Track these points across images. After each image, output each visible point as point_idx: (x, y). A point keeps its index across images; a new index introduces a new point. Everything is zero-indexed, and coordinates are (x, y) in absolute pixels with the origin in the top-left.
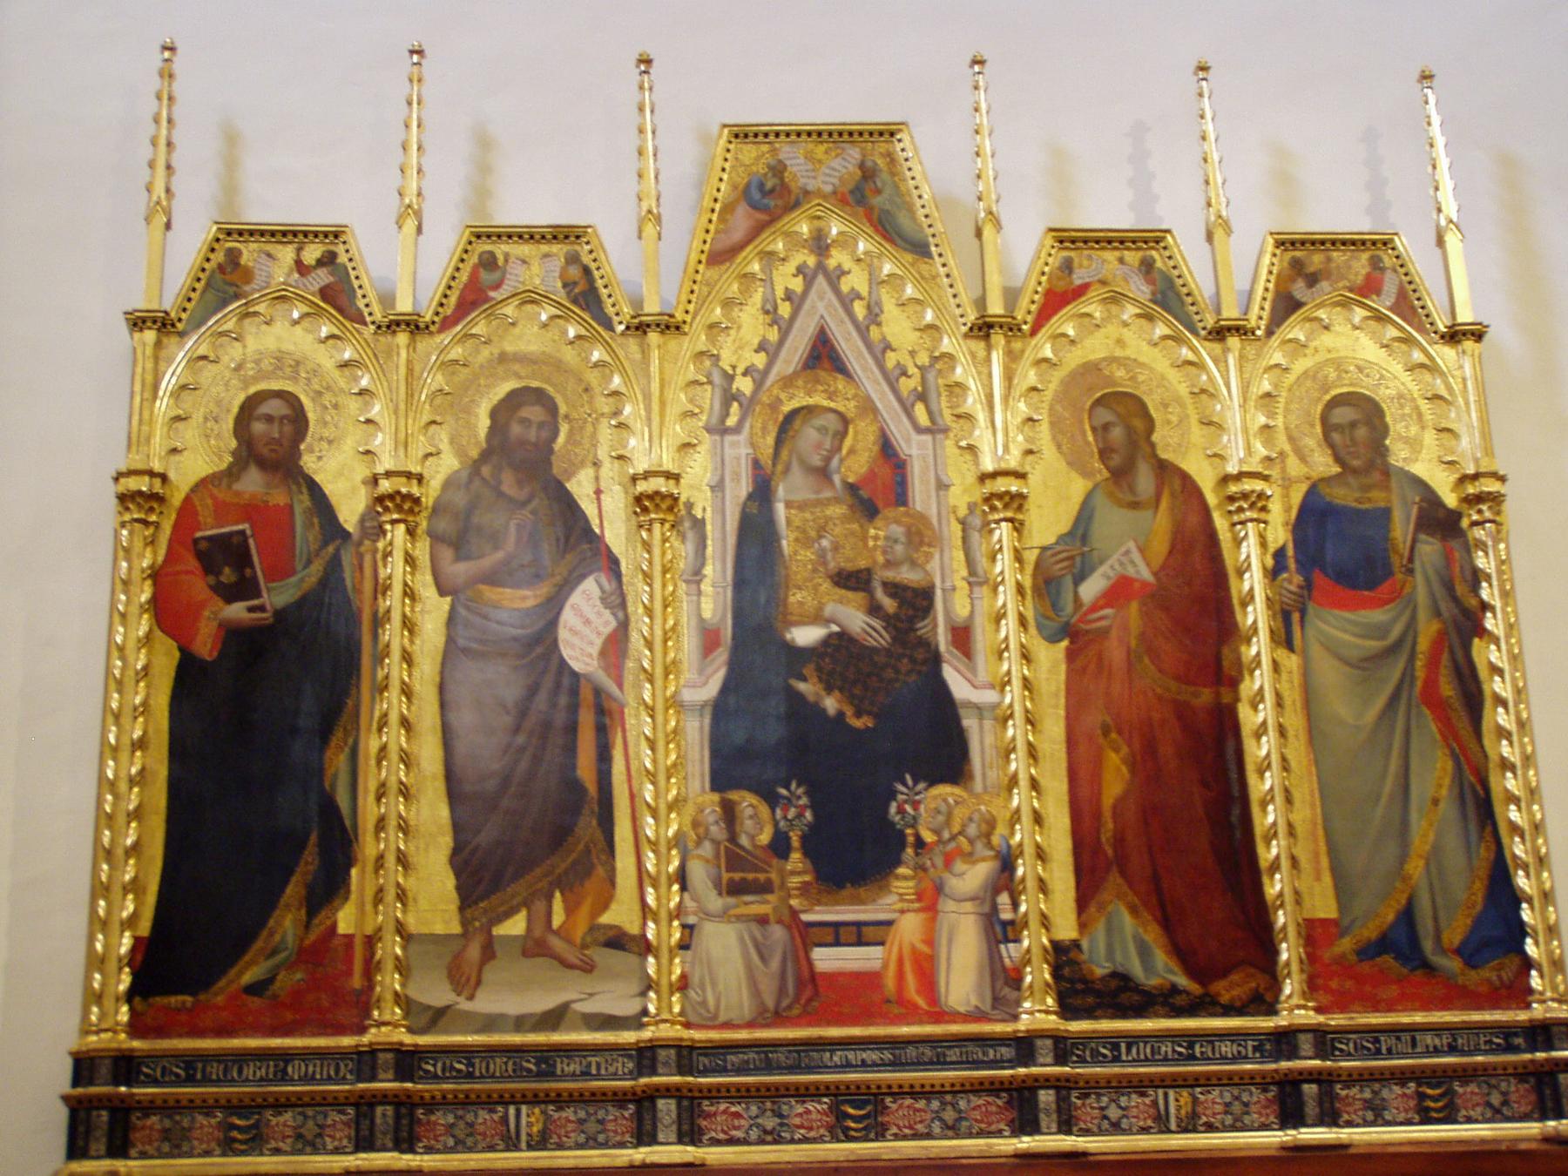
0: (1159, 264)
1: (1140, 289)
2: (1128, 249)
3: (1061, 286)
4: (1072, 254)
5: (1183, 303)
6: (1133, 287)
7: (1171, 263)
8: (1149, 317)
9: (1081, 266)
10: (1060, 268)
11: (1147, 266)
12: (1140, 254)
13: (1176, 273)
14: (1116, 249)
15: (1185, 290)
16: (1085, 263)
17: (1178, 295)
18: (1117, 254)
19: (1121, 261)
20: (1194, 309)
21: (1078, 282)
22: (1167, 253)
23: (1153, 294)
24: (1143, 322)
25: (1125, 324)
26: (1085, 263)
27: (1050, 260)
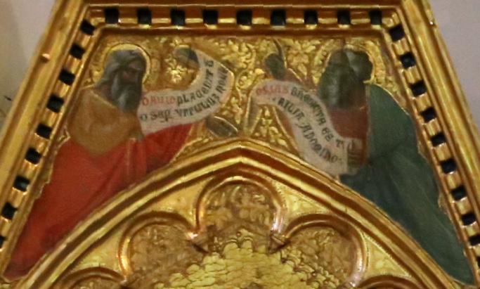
0: (379, 74)
1: (318, 144)
2: (300, 34)
3: (102, 137)
4: (142, 48)
5: (436, 187)
6: (301, 142)
7: (411, 75)
8: (343, 229)
9: (163, 81)
10: (105, 87)
11: (348, 84)
12: (330, 46)
13: (423, 101)
14: (260, 32)
15: (442, 152)
16: (176, 73)
17: (423, 162)
18: (266, 46)
19: (275, 67)
20: (463, 205)
21: (150, 127)
22: (401, 48)
23: (355, 158)
24: (327, 239)
25: (277, 246)
26: (176, 73)
27: (77, 67)
